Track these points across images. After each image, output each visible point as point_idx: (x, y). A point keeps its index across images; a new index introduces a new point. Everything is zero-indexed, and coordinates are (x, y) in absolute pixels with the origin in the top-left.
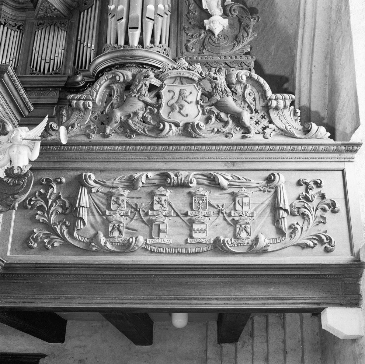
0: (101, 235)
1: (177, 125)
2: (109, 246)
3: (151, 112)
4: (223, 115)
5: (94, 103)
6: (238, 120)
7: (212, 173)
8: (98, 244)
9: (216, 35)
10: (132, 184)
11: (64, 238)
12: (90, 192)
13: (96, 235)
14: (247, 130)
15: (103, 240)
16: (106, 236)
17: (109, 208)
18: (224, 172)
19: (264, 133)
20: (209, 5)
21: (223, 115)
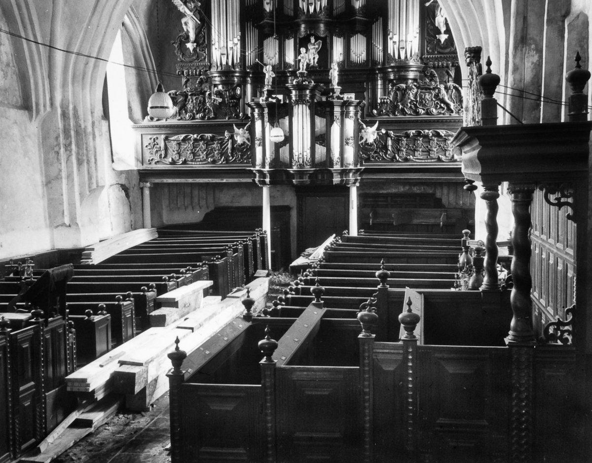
0: (396, 155)
1: (424, 110)
2: (400, 160)
3: (414, 104)
4: (442, 105)
5: (390, 100)
6: (448, 105)
7: (438, 131)
8: (396, 159)
9: (442, 42)
10: (407, 136)
11: (383, 157)
12: (391, 139)
13: (395, 155)
14: (452, 112)
15: (398, 158)
16: (398, 156)
17: (399, 145)
18: (443, 130)
19: (459, 113)
20: (439, 24)
21: (442, 105)
